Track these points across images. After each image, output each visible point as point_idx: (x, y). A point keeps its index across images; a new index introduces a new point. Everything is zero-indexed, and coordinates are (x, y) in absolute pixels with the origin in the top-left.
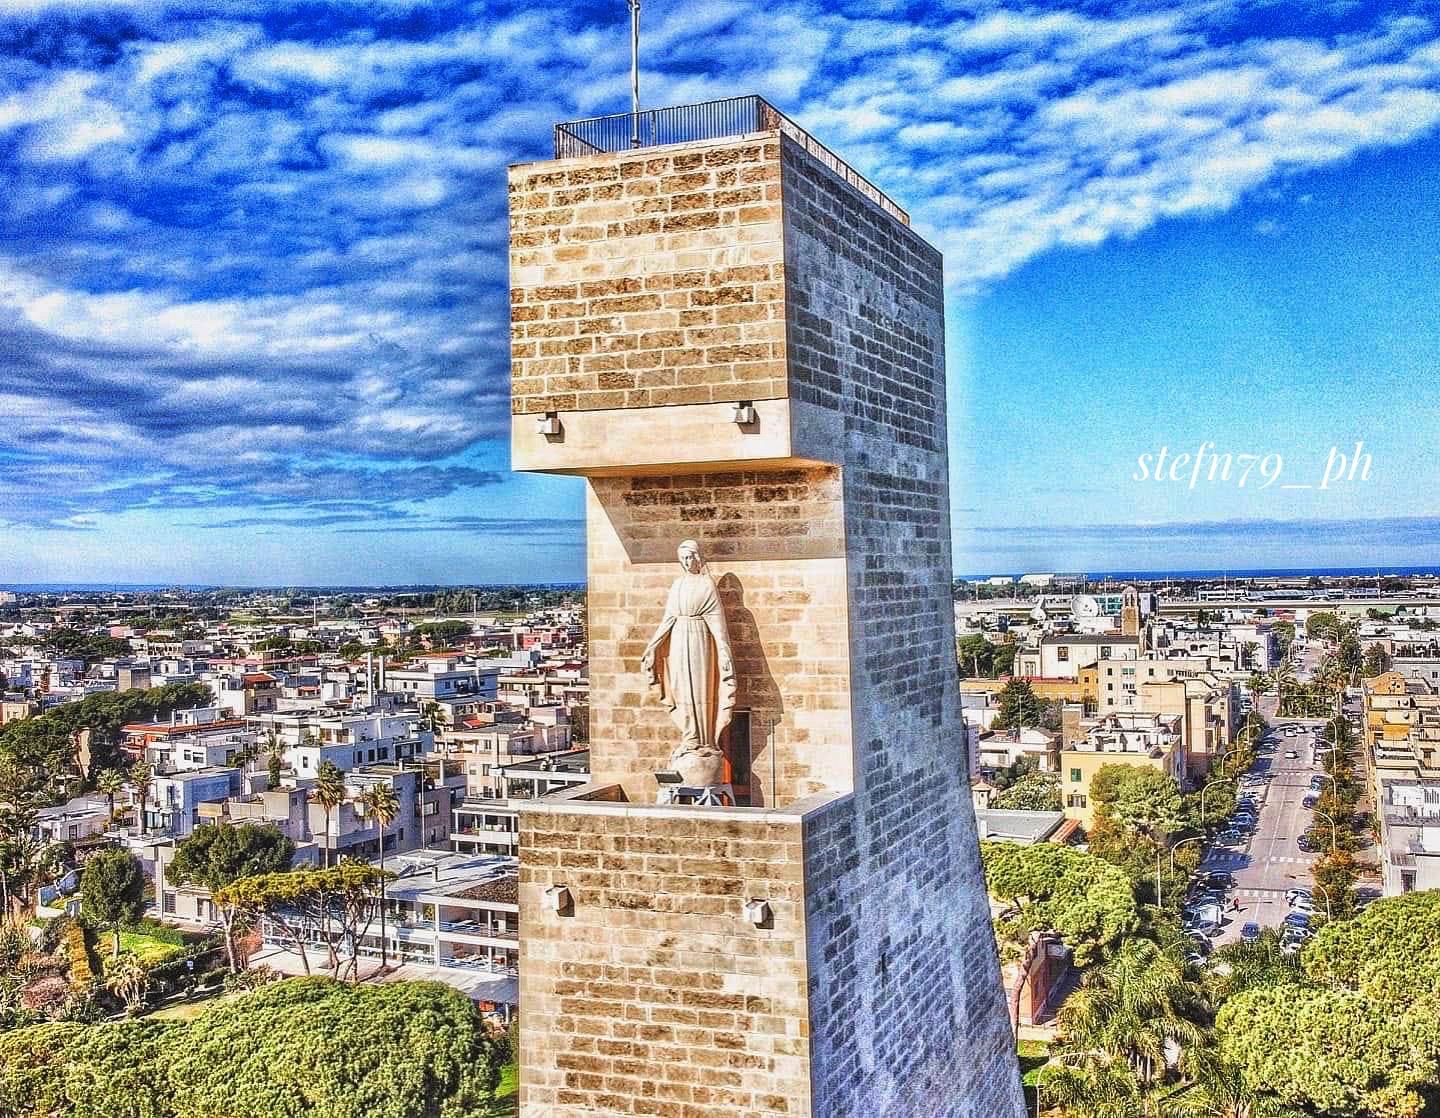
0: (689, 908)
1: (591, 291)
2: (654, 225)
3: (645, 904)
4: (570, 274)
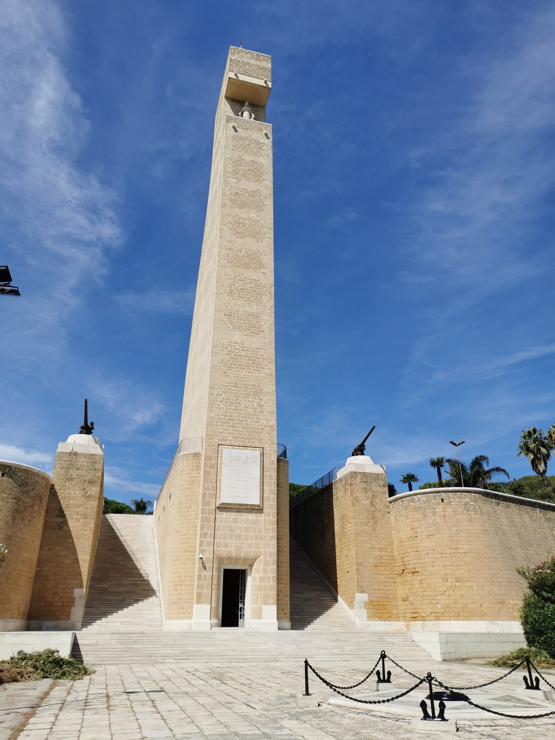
0: (254, 131)
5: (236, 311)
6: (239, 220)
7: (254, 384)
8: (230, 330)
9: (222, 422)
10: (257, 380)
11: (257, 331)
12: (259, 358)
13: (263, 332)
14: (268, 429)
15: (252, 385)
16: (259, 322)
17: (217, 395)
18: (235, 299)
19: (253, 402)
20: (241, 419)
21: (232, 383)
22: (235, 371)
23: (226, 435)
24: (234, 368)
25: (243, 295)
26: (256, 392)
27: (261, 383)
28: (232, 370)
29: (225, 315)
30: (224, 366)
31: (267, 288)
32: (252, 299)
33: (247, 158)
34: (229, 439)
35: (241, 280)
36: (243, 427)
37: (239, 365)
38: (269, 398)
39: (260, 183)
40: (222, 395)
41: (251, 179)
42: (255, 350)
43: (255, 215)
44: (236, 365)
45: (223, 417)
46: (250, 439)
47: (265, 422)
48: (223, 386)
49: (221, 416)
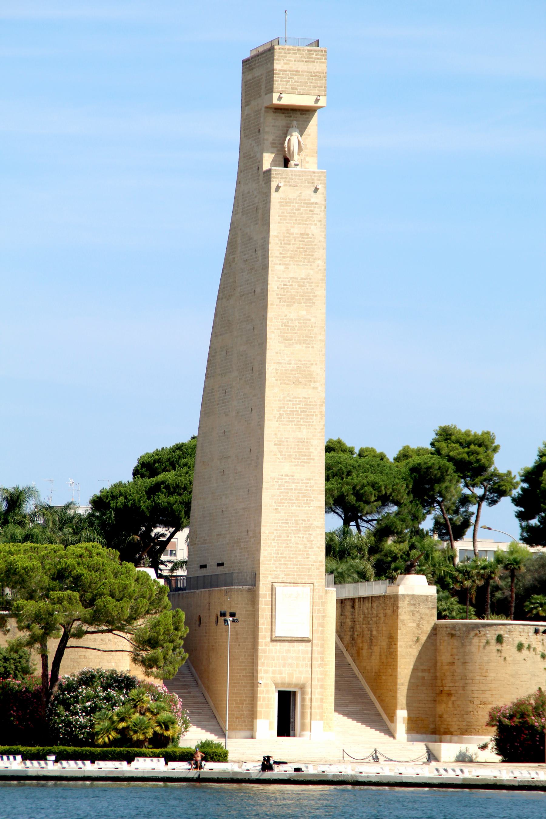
1: (290, 71)
2: (303, 61)
3: (297, 186)
4: (286, 67)
5: (285, 438)
6: (288, 322)
7: (303, 519)
8: (280, 462)
9: (275, 561)
10: (307, 514)
11: (308, 459)
12: (308, 490)
13: (313, 459)
14: (317, 564)
15: (302, 520)
16: (308, 449)
17: (269, 533)
18: (284, 425)
19: (303, 537)
20: (291, 556)
21: (283, 520)
22: (286, 506)
23: (279, 572)
24: (284, 503)
25: (292, 418)
26: (306, 527)
27: (311, 517)
28: (283, 506)
29: (275, 445)
30: (275, 502)
31: (318, 407)
32: (302, 423)
33: (295, 230)
34: (281, 576)
35: (290, 401)
36: (294, 565)
37: (290, 500)
38: (318, 532)
39: (311, 265)
40: (273, 533)
41: (301, 261)
42: (305, 481)
43: (304, 313)
44: (286, 499)
45: (275, 556)
46: (300, 575)
47: (314, 557)
48: (275, 523)
49: (273, 555)
